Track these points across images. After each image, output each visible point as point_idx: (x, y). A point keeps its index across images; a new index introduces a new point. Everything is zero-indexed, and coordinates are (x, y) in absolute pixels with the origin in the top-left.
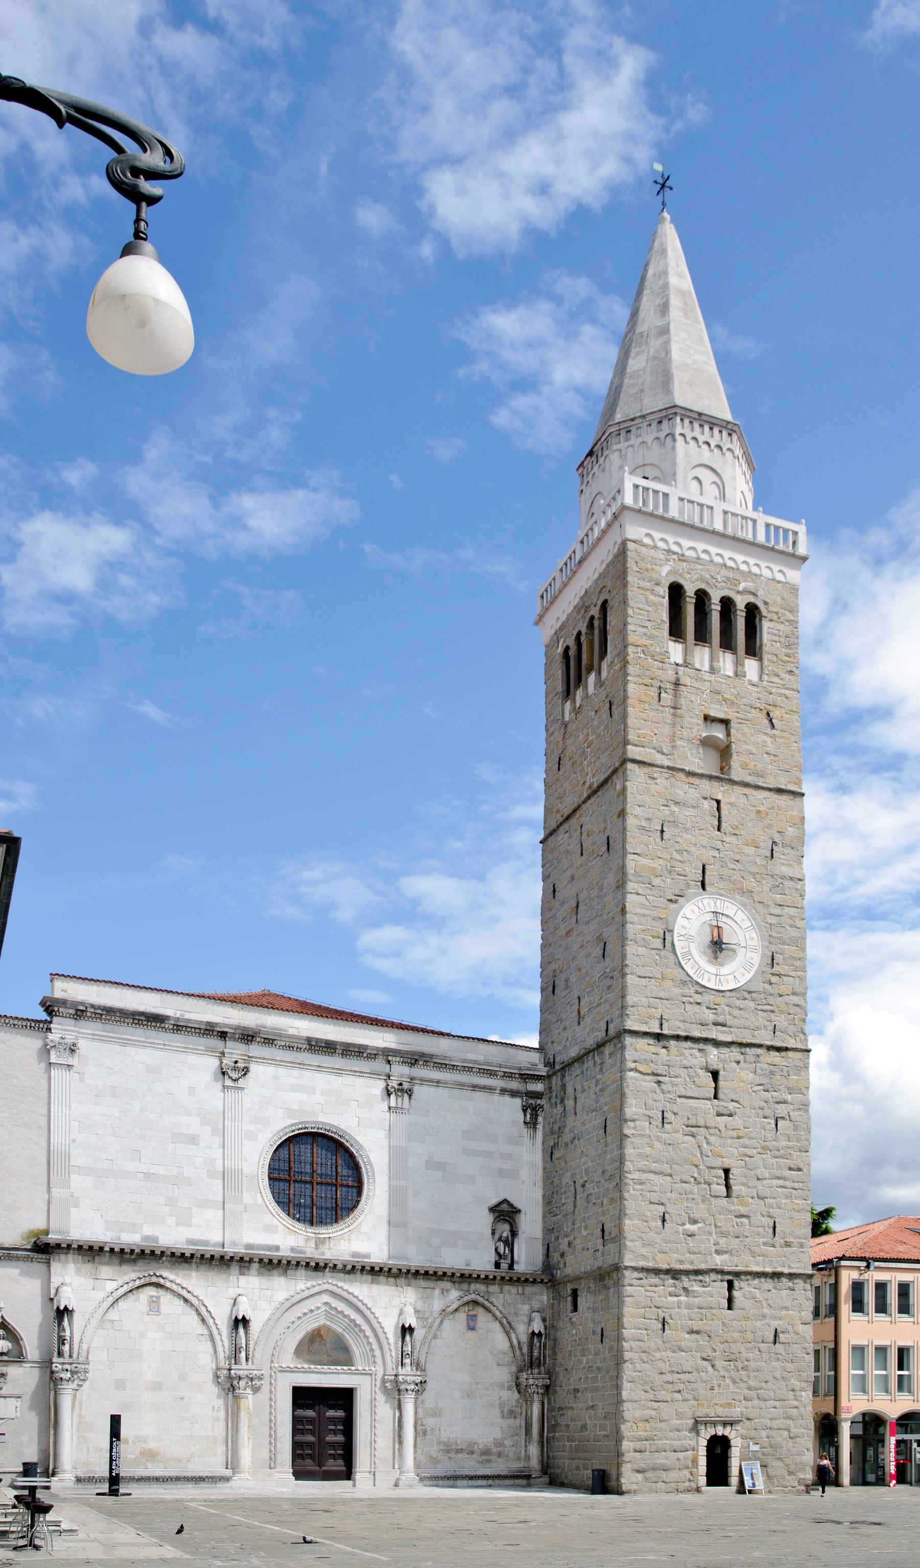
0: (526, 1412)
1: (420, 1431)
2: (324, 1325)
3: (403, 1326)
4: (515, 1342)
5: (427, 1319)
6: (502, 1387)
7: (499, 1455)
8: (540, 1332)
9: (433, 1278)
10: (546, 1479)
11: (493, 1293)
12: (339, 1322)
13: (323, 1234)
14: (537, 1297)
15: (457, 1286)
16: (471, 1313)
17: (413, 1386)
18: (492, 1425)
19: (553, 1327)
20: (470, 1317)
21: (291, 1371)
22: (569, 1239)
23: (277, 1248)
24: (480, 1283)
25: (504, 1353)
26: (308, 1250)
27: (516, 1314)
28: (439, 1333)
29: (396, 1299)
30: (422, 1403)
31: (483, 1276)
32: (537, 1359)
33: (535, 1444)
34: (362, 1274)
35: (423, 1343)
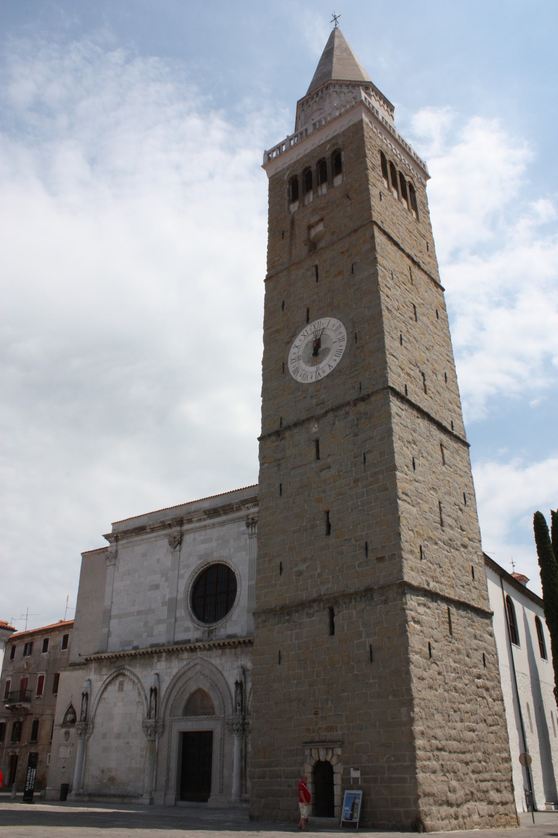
13: (213, 626)
23: (189, 641)
29: (236, 663)
34: (216, 649)
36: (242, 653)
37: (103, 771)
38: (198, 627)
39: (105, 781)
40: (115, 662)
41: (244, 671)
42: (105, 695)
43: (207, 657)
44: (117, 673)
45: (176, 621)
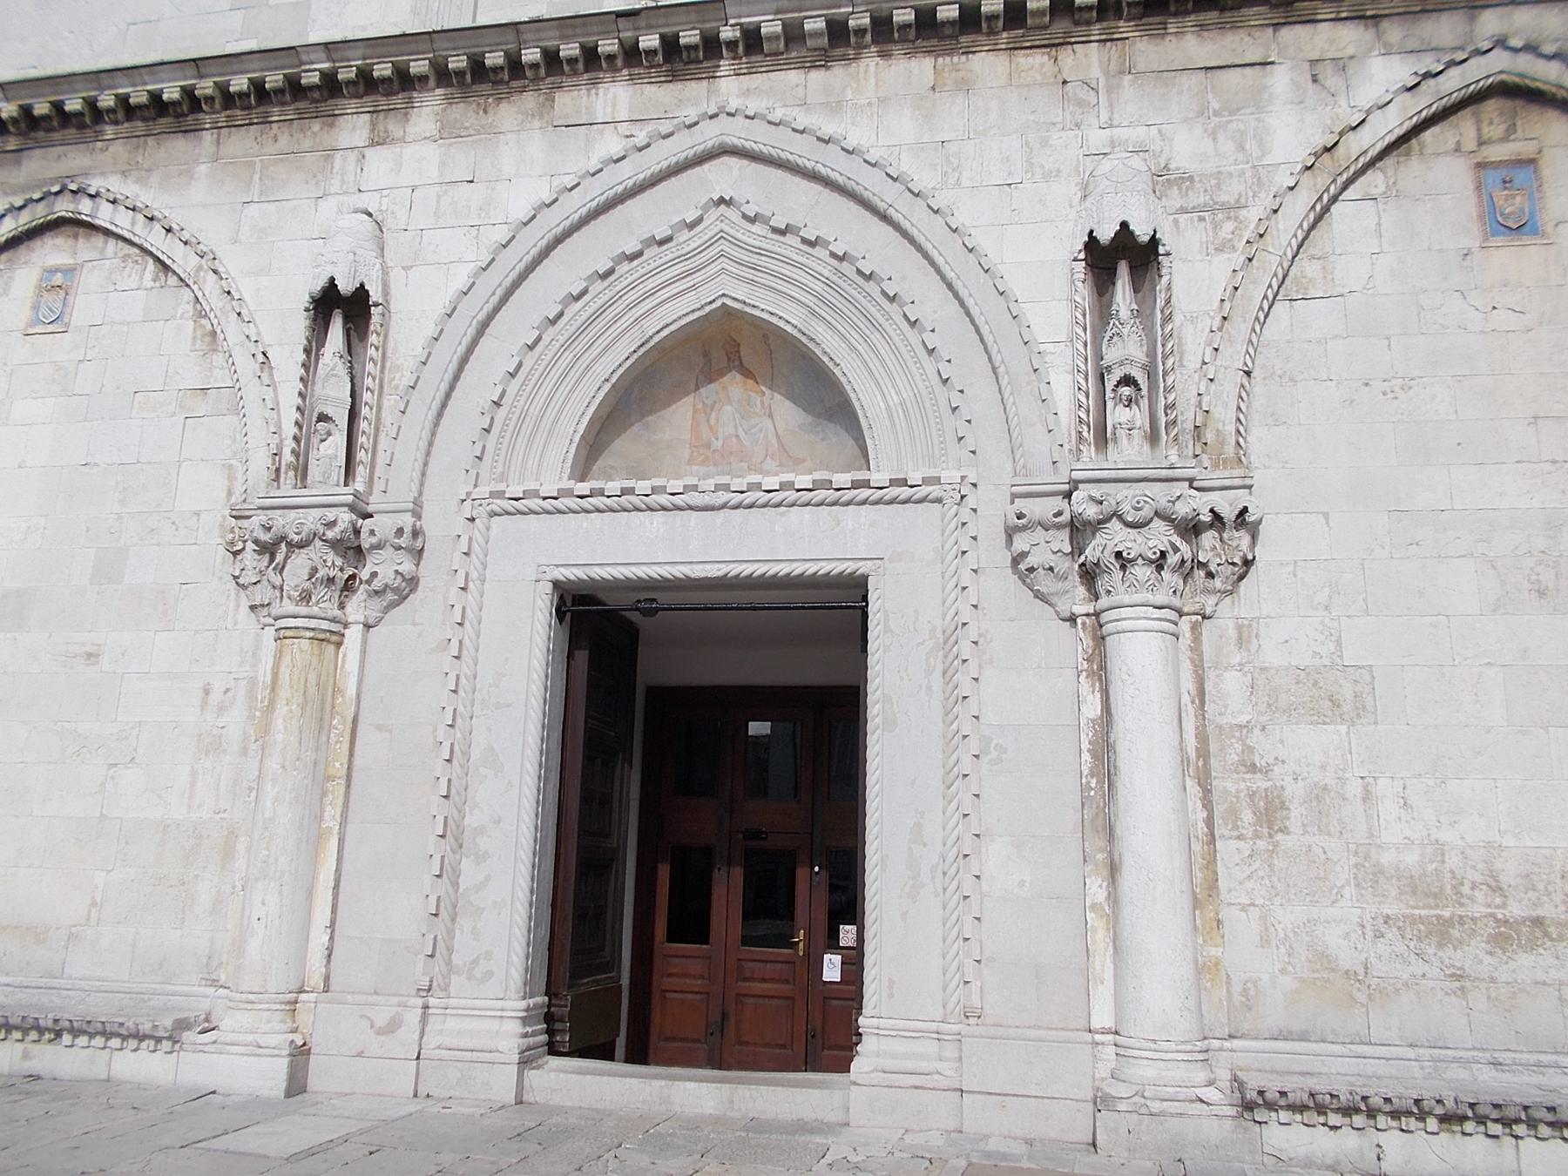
3: (1092, 244)
5: (1239, 206)
12: (788, 280)
17: (1160, 536)
20: (1492, 177)
21: (552, 506)
34: (885, 55)
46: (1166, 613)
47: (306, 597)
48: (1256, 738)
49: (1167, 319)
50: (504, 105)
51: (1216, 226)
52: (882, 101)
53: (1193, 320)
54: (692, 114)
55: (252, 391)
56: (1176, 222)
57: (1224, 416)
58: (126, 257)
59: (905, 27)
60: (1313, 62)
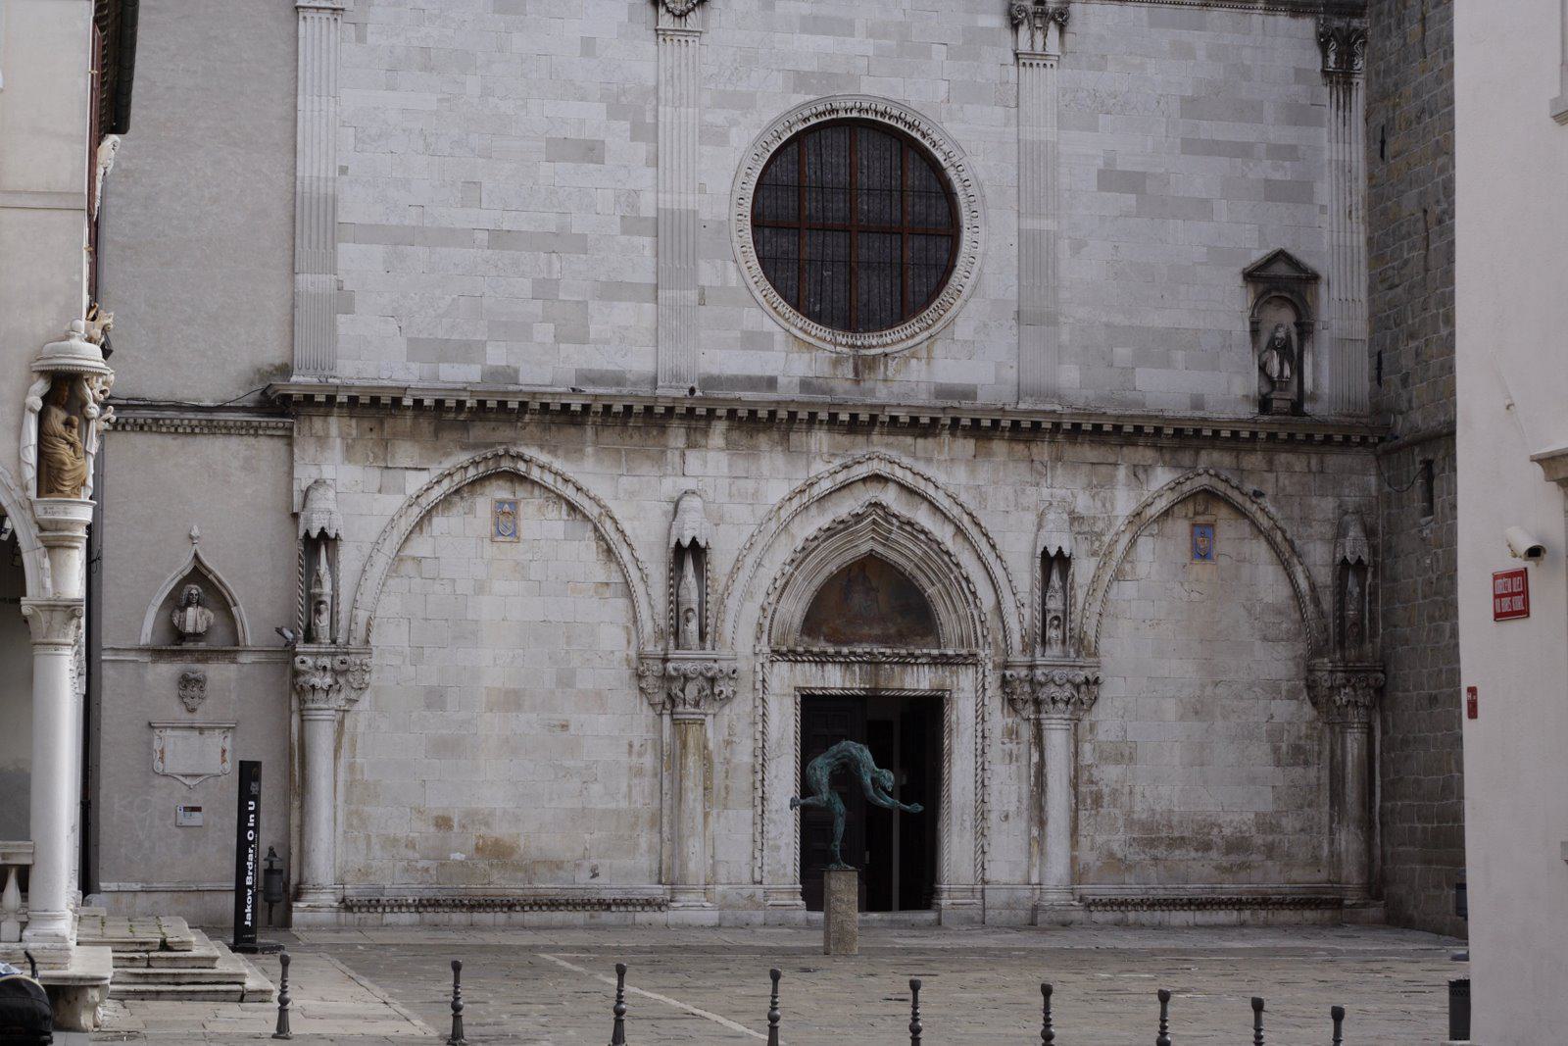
0: (1332, 751)
1: (1085, 795)
2: (871, 556)
3: (1045, 552)
4: (1303, 584)
5: (1100, 535)
6: (1273, 689)
7: (1270, 850)
8: (1360, 561)
9: (1114, 440)
10: (1375, 912)
11: (1251, 472)
13: (871, 347)
14: (1354, 477)
15: (1167, 457)
16: (1201, 519)
18: (1253, 780)
19: (1389, 549)
20: (1198, 530)
22: (1417, 343)
23: (771, 383)
24: (1221, 449)
25: (1280, 613)
26: (835, 384)
27: (1305, 521)
28: (1127, 567)
29: (1030, 490)
30: (1091, 730)
31: (1225, 434)
32: (1355, 624)
33: (1352, 828)
34: (953, 434)
35: (1092, 591)
36: (1059, 459)
37: (443, 823)
38: (800, 335)
39: (458, 856)
40: (465, 426)
41: (1075, 518)
42: (420, 547)
43: (914, 456)
44: (482, 468)
45: (702, 302)
46: (1068, 722)
47: (697, 704)
48: (1095, 772)
49: (1072, 588)
50: (761, 435)
51: (1092, 543)
52: (952, 459)
53: (1081, 587)
54: (858, 453)
55: (639, 589)
56: (1076, 538)
57: (1091, 634)
58: (547, 499)
59: (964, 427)
60: (1135, 466)
